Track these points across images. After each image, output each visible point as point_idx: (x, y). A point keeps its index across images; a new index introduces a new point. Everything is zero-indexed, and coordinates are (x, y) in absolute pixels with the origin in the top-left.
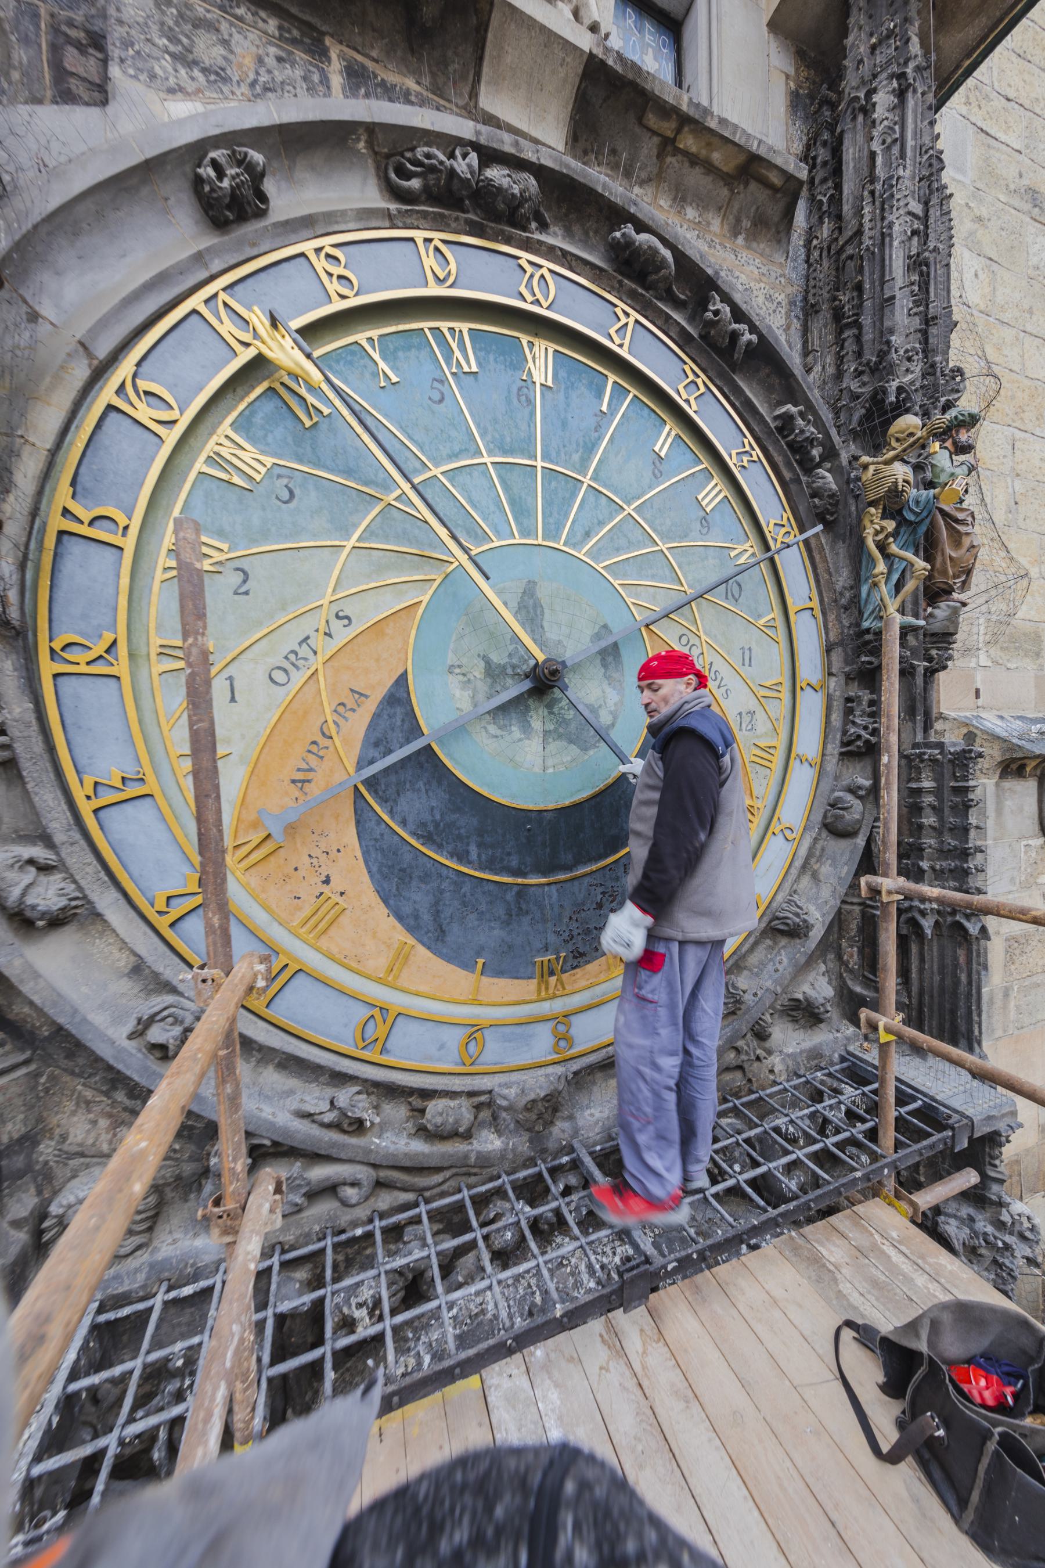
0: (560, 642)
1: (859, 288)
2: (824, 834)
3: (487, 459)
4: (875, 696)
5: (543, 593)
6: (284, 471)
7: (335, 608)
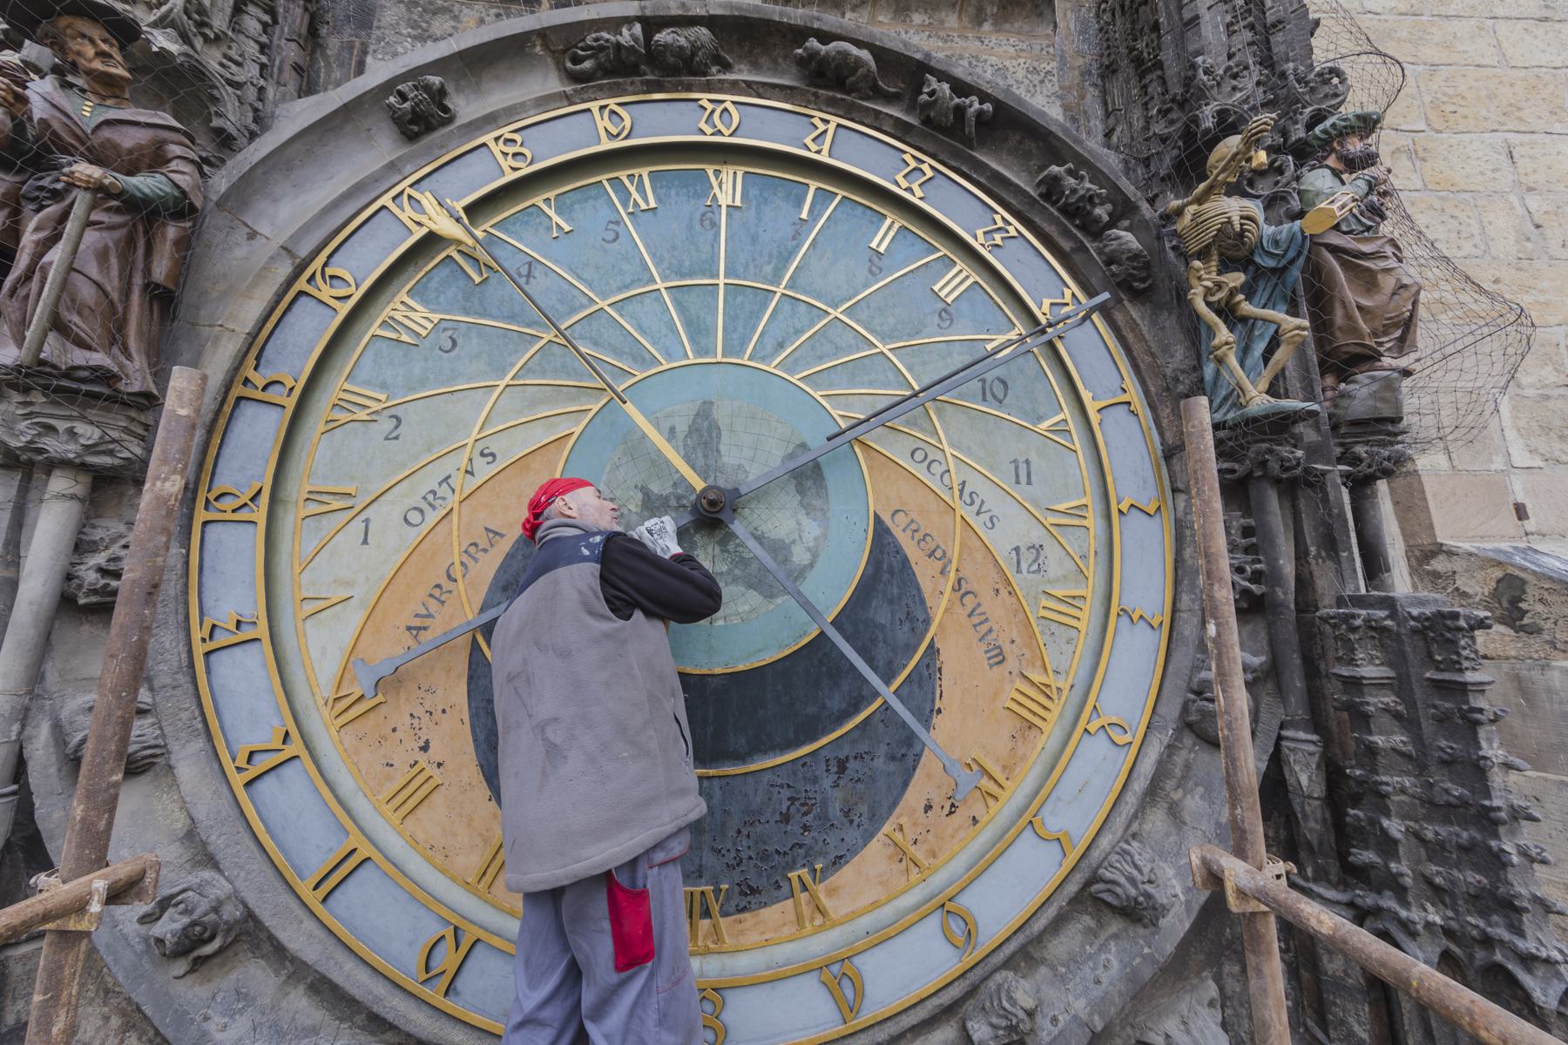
0: (740, 466)
1: (1156, 27)
2: (1188, 740)
3: (660, 285)
5: (721, 415)
6: (449, 325)
7: (480, 446)
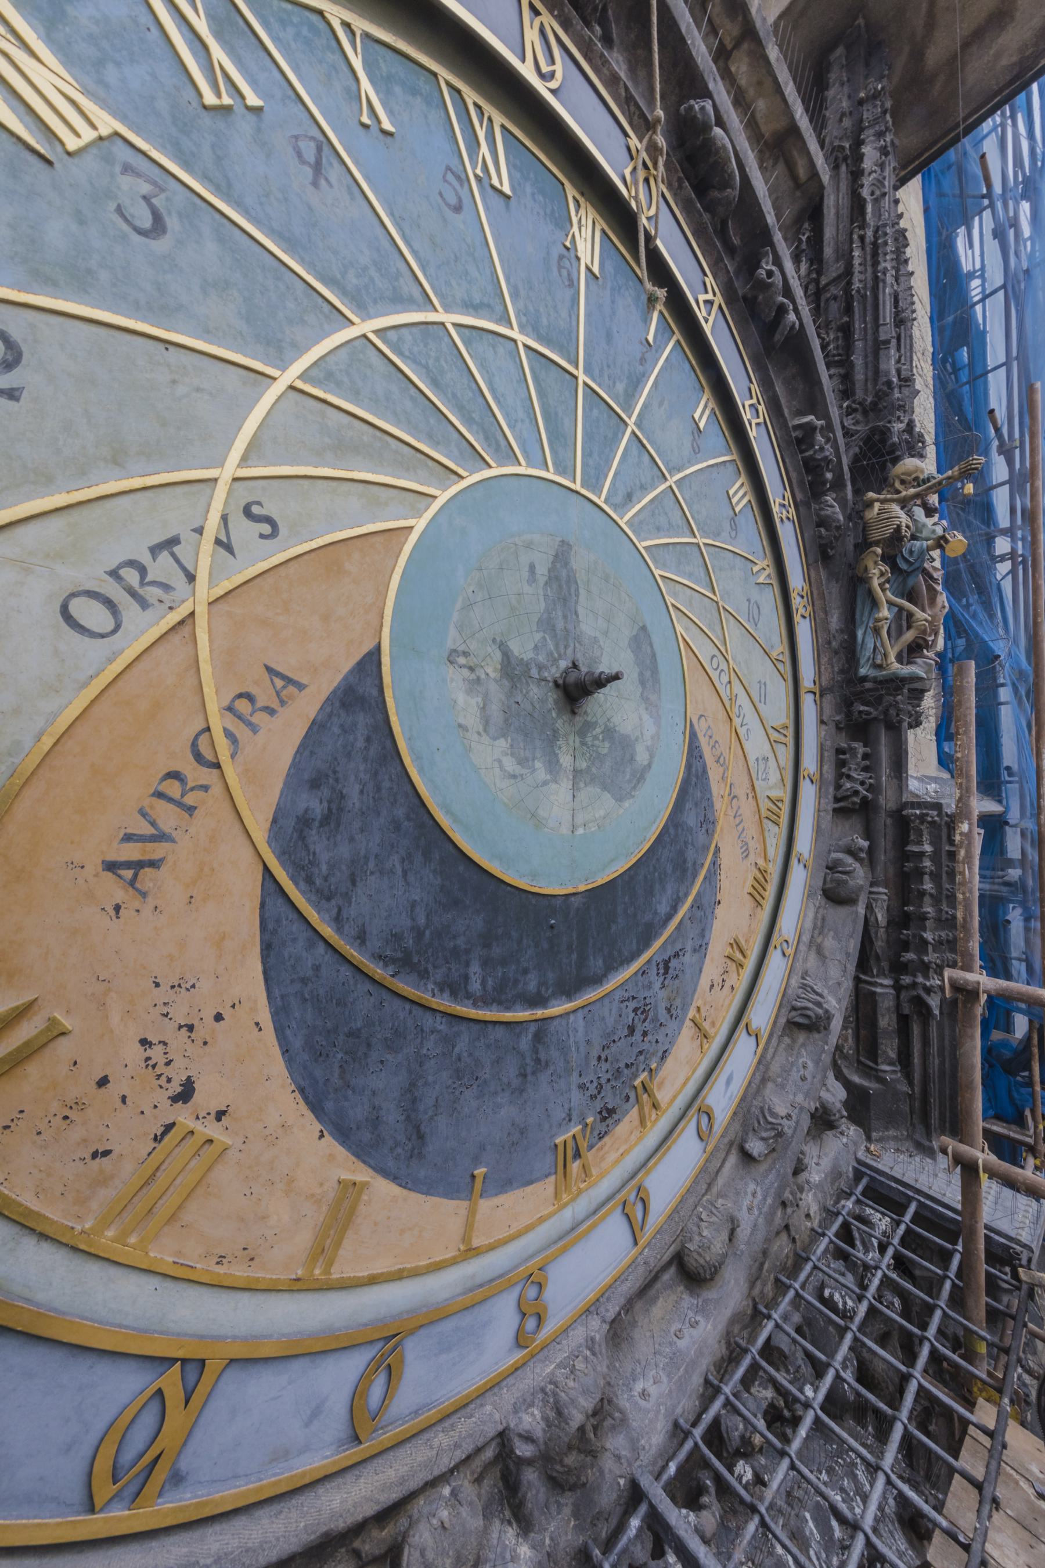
0: (596, 640)
4: (868, 750)
7: (244, 494)
